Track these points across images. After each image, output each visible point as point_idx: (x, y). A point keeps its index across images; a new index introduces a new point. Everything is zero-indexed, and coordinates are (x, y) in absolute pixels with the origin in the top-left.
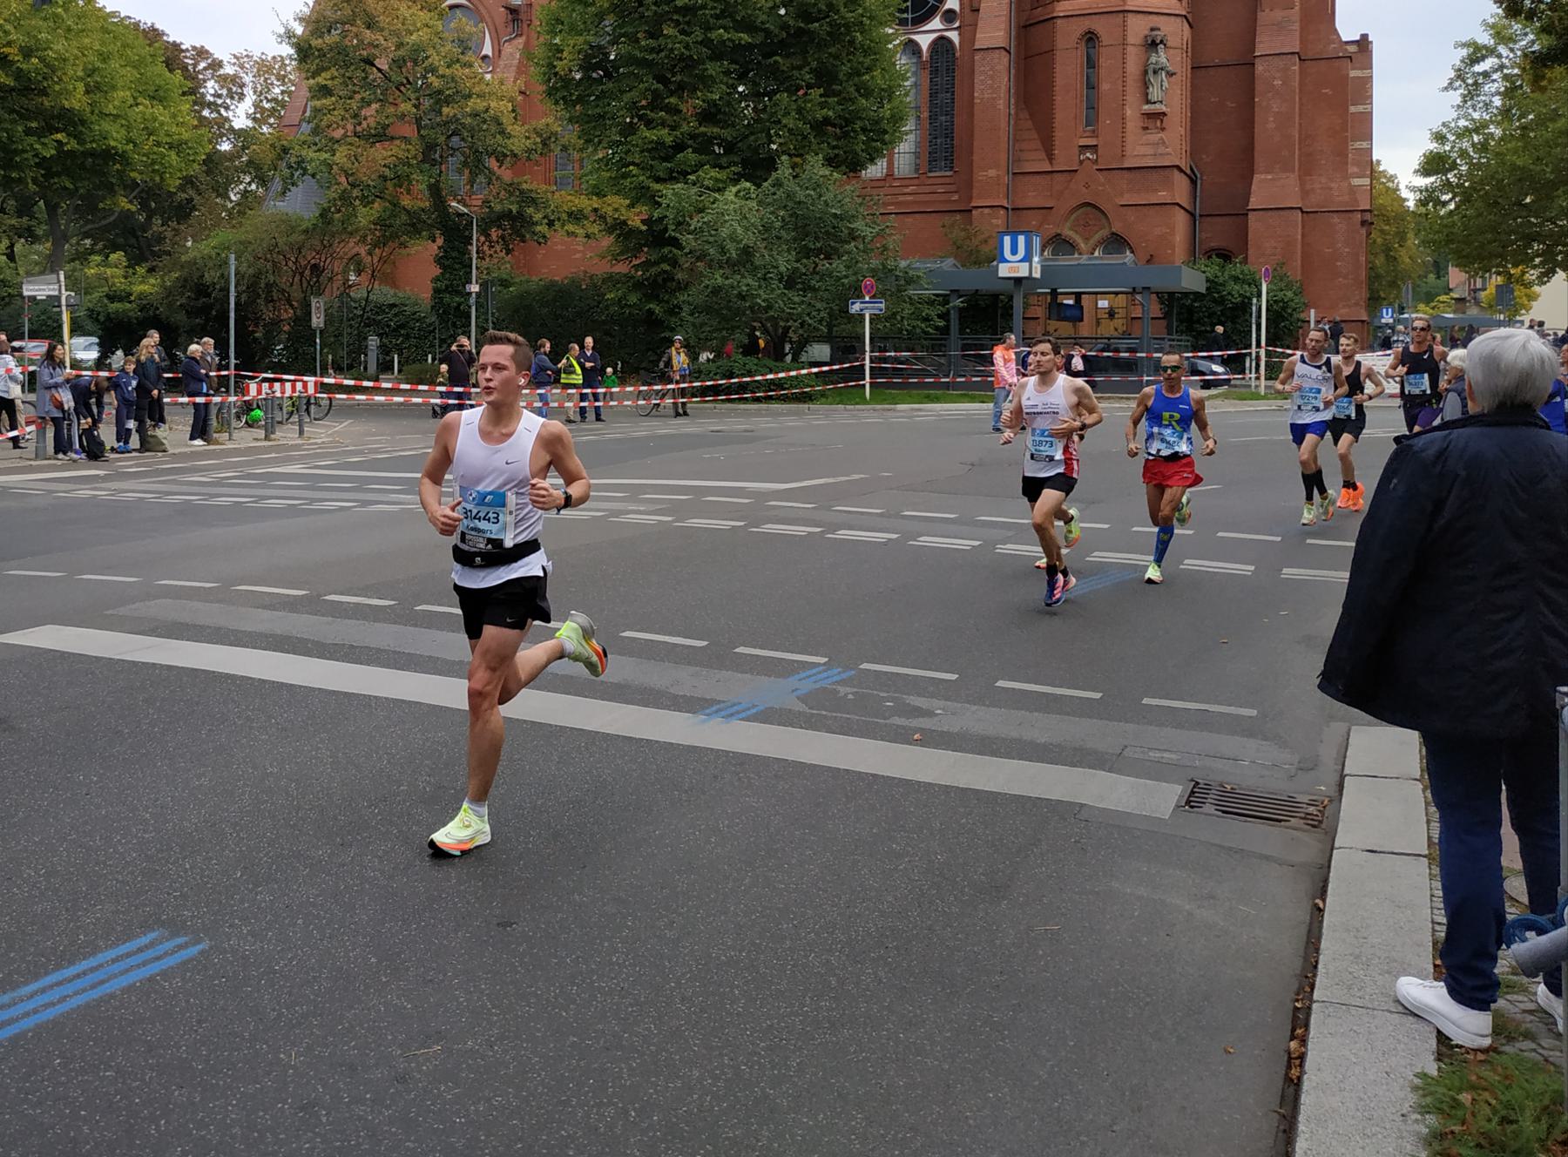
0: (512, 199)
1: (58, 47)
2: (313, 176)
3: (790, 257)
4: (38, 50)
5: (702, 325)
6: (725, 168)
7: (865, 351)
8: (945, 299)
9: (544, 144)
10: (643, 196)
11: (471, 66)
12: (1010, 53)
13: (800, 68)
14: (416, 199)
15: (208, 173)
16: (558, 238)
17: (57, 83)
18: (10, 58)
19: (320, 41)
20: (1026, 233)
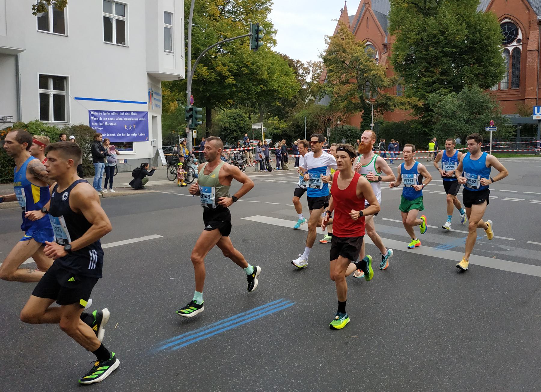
0: (384, 99)
1: (261, 62)
2: (328, 95)
3: (467, 114)
4: (255, 63)
5: (440, 135)
7: (490, 142)
8: (516, 126)
9: (393, 83)
11: (372, 62)
12: (538, 51)
13: (471, 58)
14: (356, 100)
15: (300, 94)
16: (397, 110)
18: (248, 65)
19: (330, 57)
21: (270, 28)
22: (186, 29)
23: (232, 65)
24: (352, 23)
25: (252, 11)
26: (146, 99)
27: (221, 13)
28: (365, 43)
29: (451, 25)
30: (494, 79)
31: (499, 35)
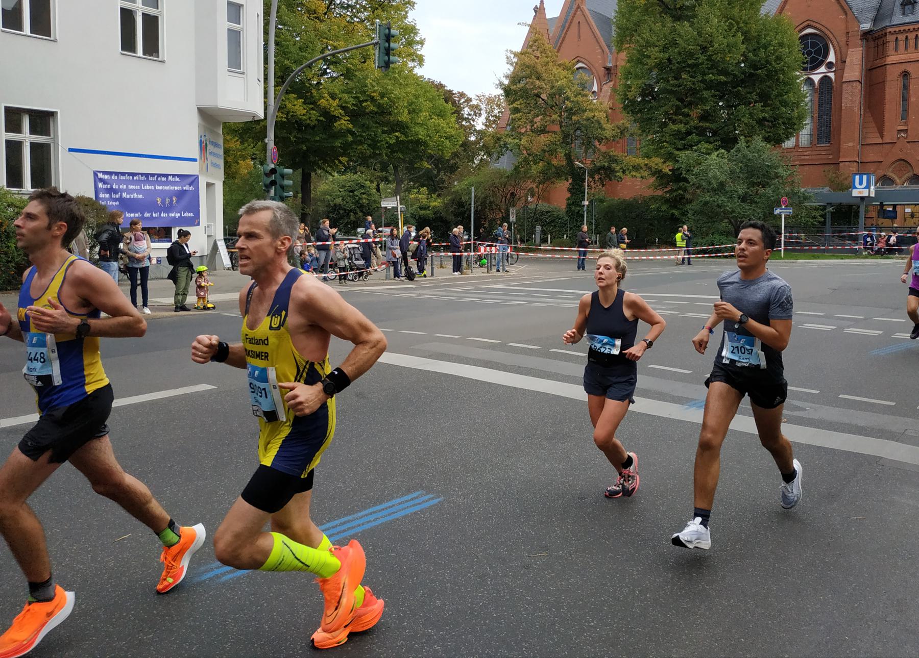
0: (605, 160)
2: (511, 151)
5: (698, 220)
6: (712, 143)
8: (824, 208)
9: (621, 133)
10: (670, 157)
11: (586, 96)
13: (752, 93)
14: (559, 161)
15: (465, 151)
16: (627, 178)
17: (395, 109)
18: (375, 98)
19: (515, 86)
20: (868, 174)
21: (412, 35)
22: (266, 33)
23: (346, 96)
24: (553, 30)
25: (381, 5)
26: (196, 154)
27: (328, 8)
28: (574, 65)
29: (717, 37)
30: (788, 128)
31: (796, 54)
